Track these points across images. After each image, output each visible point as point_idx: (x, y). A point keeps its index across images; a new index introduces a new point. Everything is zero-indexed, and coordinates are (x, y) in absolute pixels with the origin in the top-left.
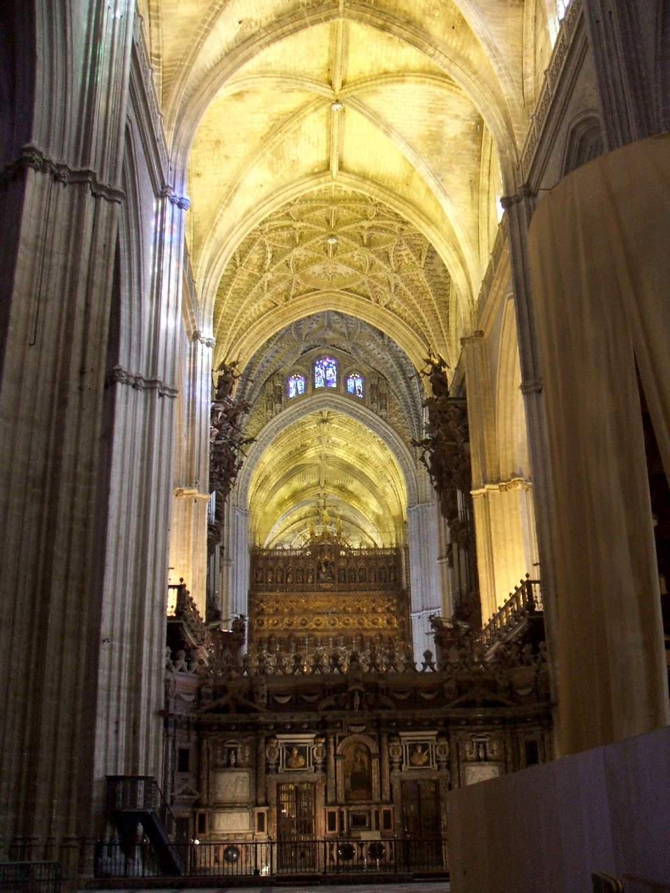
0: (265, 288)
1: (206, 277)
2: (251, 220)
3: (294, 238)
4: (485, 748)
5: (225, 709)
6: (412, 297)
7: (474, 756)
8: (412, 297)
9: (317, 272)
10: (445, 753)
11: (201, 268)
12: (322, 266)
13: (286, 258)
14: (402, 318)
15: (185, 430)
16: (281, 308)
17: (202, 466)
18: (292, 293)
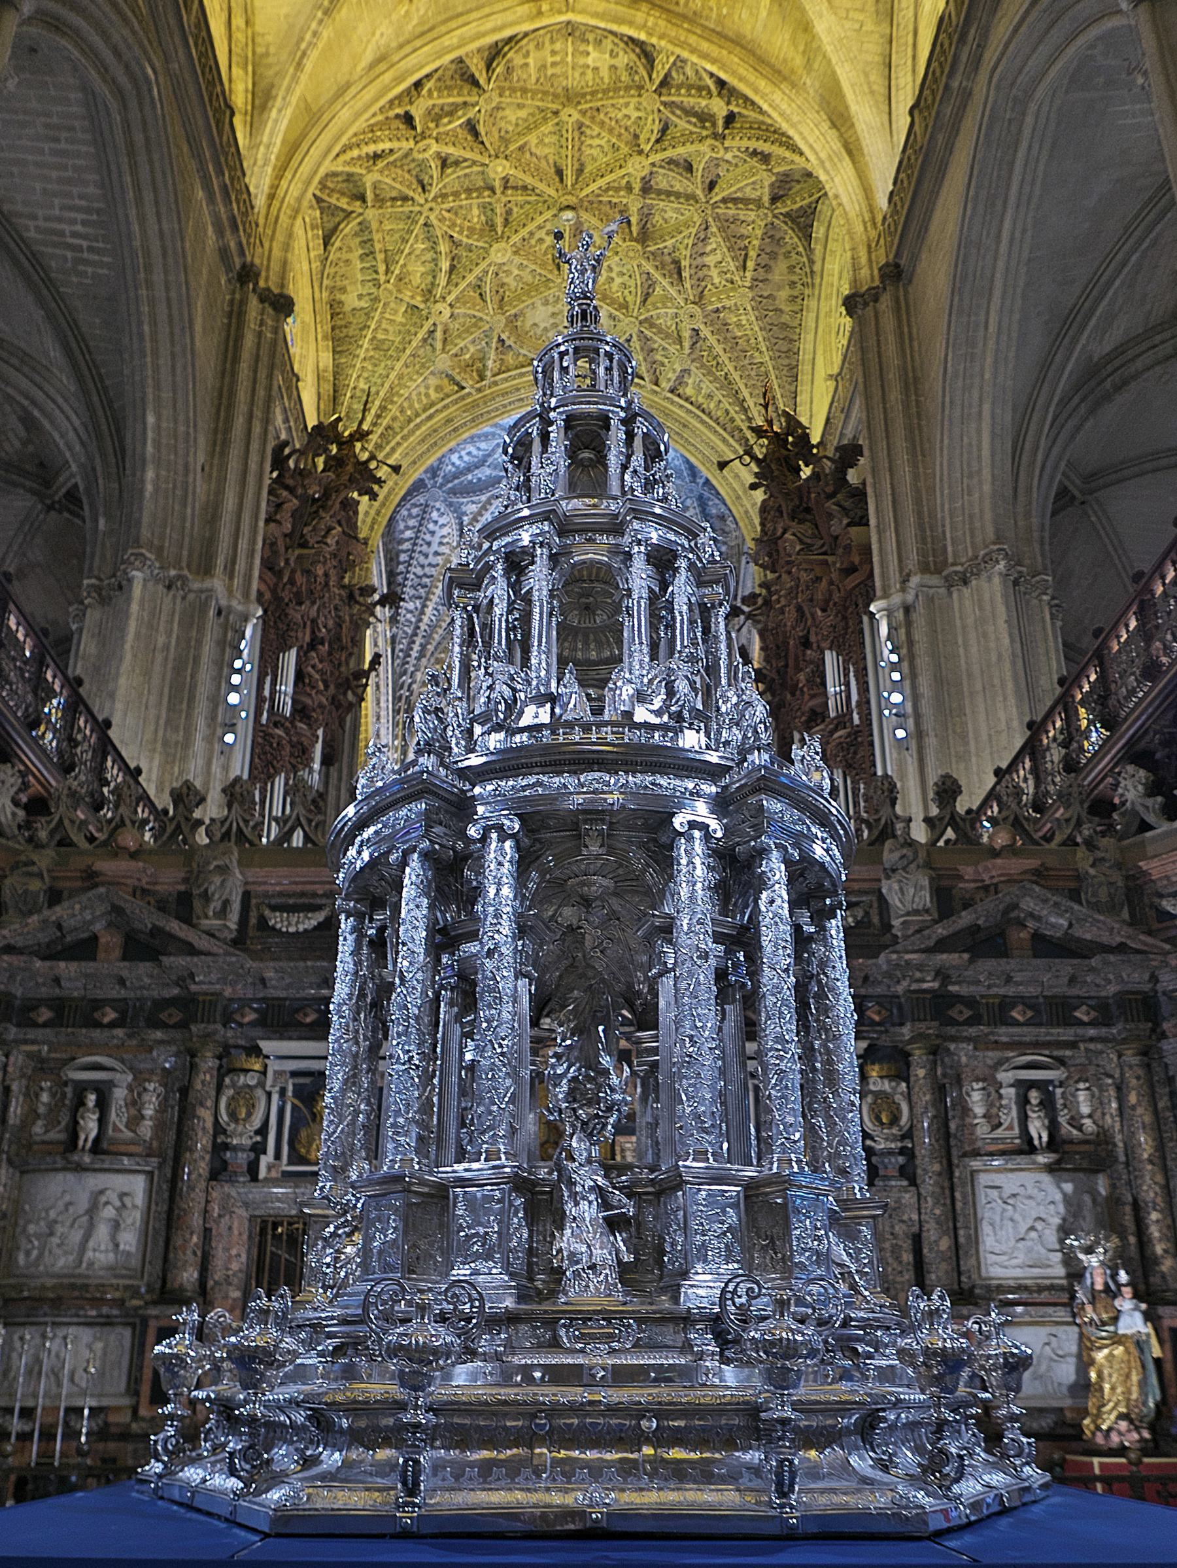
0: (439, 345)
1: (279, 177)
2: (387, 77)
3: (492, 227)
4: (1048, 1104)
5: (85, 949)
6: (724, 358)
7: (1009, 1132)
8: (724, 358)
9: (542, 325)
10: (895, 1120)
11: (268, 146)
12: (551, 309)
13: (478, 271)
14: (703, 411)
15: (201, 458)
16: (469, 394)
17: (243, 544)
18: (490, 363)
